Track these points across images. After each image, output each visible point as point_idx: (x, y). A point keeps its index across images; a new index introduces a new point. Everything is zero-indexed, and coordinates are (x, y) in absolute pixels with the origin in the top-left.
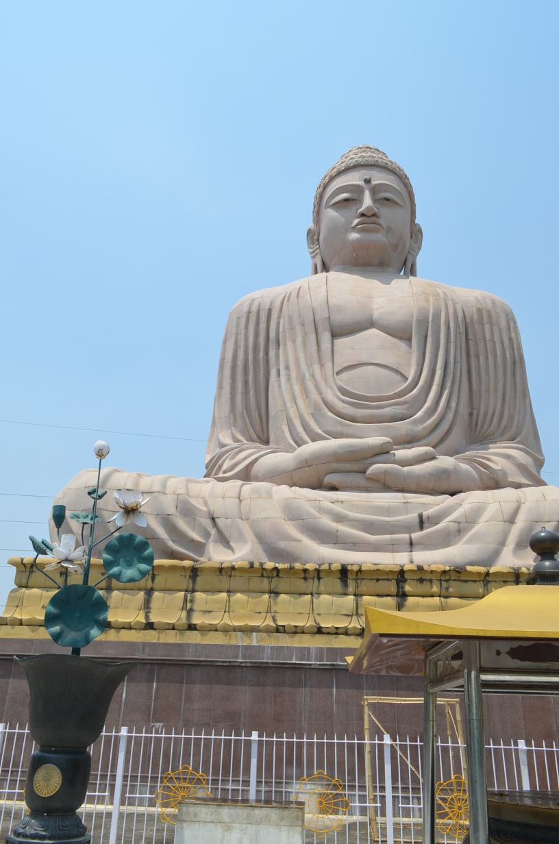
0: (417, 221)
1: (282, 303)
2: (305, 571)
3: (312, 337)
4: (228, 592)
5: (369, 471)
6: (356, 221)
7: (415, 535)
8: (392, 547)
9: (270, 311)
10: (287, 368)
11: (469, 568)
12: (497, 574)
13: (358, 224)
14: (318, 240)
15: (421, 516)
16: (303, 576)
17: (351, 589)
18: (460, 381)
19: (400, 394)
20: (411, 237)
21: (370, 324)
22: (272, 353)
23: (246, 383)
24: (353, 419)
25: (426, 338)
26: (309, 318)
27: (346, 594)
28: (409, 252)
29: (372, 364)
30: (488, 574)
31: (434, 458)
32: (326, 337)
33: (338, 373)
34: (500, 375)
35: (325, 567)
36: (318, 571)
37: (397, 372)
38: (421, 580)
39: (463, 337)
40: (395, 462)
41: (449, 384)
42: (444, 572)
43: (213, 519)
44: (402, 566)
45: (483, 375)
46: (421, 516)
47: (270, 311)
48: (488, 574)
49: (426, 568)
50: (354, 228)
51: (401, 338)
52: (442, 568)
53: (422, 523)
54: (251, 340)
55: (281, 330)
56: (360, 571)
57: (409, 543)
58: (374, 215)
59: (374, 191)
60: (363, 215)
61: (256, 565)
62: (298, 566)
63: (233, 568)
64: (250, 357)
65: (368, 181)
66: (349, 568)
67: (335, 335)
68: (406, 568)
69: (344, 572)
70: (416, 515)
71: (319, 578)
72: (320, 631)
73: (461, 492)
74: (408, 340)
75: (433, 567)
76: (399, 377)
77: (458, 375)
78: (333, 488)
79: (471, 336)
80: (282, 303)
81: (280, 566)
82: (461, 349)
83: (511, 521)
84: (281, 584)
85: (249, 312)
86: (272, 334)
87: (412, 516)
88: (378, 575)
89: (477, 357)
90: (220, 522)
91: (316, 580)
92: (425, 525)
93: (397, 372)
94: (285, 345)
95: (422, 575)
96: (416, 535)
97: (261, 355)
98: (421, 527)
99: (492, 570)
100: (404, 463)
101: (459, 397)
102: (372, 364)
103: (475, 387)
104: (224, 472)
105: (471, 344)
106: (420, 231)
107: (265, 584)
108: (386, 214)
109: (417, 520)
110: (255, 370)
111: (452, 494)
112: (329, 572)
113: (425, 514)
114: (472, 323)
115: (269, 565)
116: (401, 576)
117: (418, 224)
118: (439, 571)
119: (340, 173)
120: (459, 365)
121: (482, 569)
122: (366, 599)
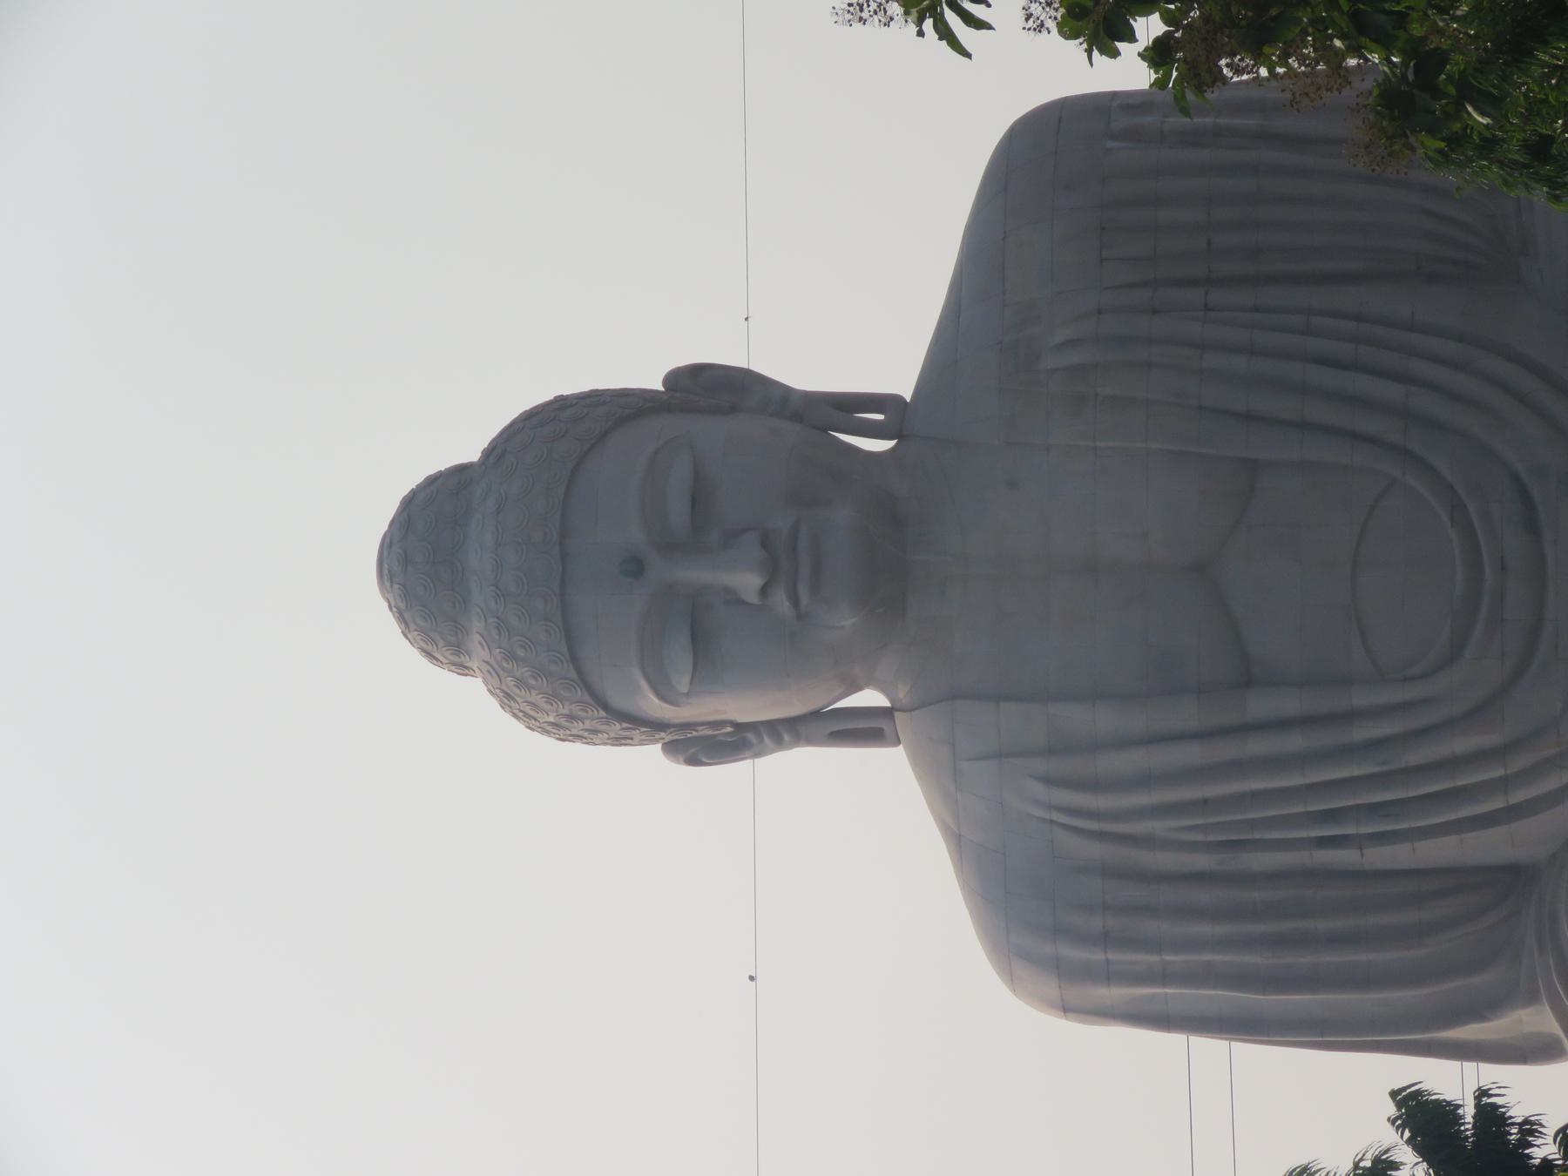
0: (652, 380)
1: (1101, 836)
3: (1257, 746)
6: (781, 602)
13: (795, 600)
14: (739, 727)
18: (1359, 318)
20: (733, 409)
23: (1336, 940)
25: (1249, 417)
26: (1192, 754)
28: (797, 417)
32: (1260, 705)
47: (1111, 872)
50: (799, 617)
55: (1199, 837)
58: (765, 542)
60: (764, 591)
65: (635, 567)
67: (1248, 678)
80: (1101, 836)
85: (1105, 939)
86: (1202, 862)
94: (1252, 824)
97: (1257, 895)
106: (697, 371)
119: (574, 659)
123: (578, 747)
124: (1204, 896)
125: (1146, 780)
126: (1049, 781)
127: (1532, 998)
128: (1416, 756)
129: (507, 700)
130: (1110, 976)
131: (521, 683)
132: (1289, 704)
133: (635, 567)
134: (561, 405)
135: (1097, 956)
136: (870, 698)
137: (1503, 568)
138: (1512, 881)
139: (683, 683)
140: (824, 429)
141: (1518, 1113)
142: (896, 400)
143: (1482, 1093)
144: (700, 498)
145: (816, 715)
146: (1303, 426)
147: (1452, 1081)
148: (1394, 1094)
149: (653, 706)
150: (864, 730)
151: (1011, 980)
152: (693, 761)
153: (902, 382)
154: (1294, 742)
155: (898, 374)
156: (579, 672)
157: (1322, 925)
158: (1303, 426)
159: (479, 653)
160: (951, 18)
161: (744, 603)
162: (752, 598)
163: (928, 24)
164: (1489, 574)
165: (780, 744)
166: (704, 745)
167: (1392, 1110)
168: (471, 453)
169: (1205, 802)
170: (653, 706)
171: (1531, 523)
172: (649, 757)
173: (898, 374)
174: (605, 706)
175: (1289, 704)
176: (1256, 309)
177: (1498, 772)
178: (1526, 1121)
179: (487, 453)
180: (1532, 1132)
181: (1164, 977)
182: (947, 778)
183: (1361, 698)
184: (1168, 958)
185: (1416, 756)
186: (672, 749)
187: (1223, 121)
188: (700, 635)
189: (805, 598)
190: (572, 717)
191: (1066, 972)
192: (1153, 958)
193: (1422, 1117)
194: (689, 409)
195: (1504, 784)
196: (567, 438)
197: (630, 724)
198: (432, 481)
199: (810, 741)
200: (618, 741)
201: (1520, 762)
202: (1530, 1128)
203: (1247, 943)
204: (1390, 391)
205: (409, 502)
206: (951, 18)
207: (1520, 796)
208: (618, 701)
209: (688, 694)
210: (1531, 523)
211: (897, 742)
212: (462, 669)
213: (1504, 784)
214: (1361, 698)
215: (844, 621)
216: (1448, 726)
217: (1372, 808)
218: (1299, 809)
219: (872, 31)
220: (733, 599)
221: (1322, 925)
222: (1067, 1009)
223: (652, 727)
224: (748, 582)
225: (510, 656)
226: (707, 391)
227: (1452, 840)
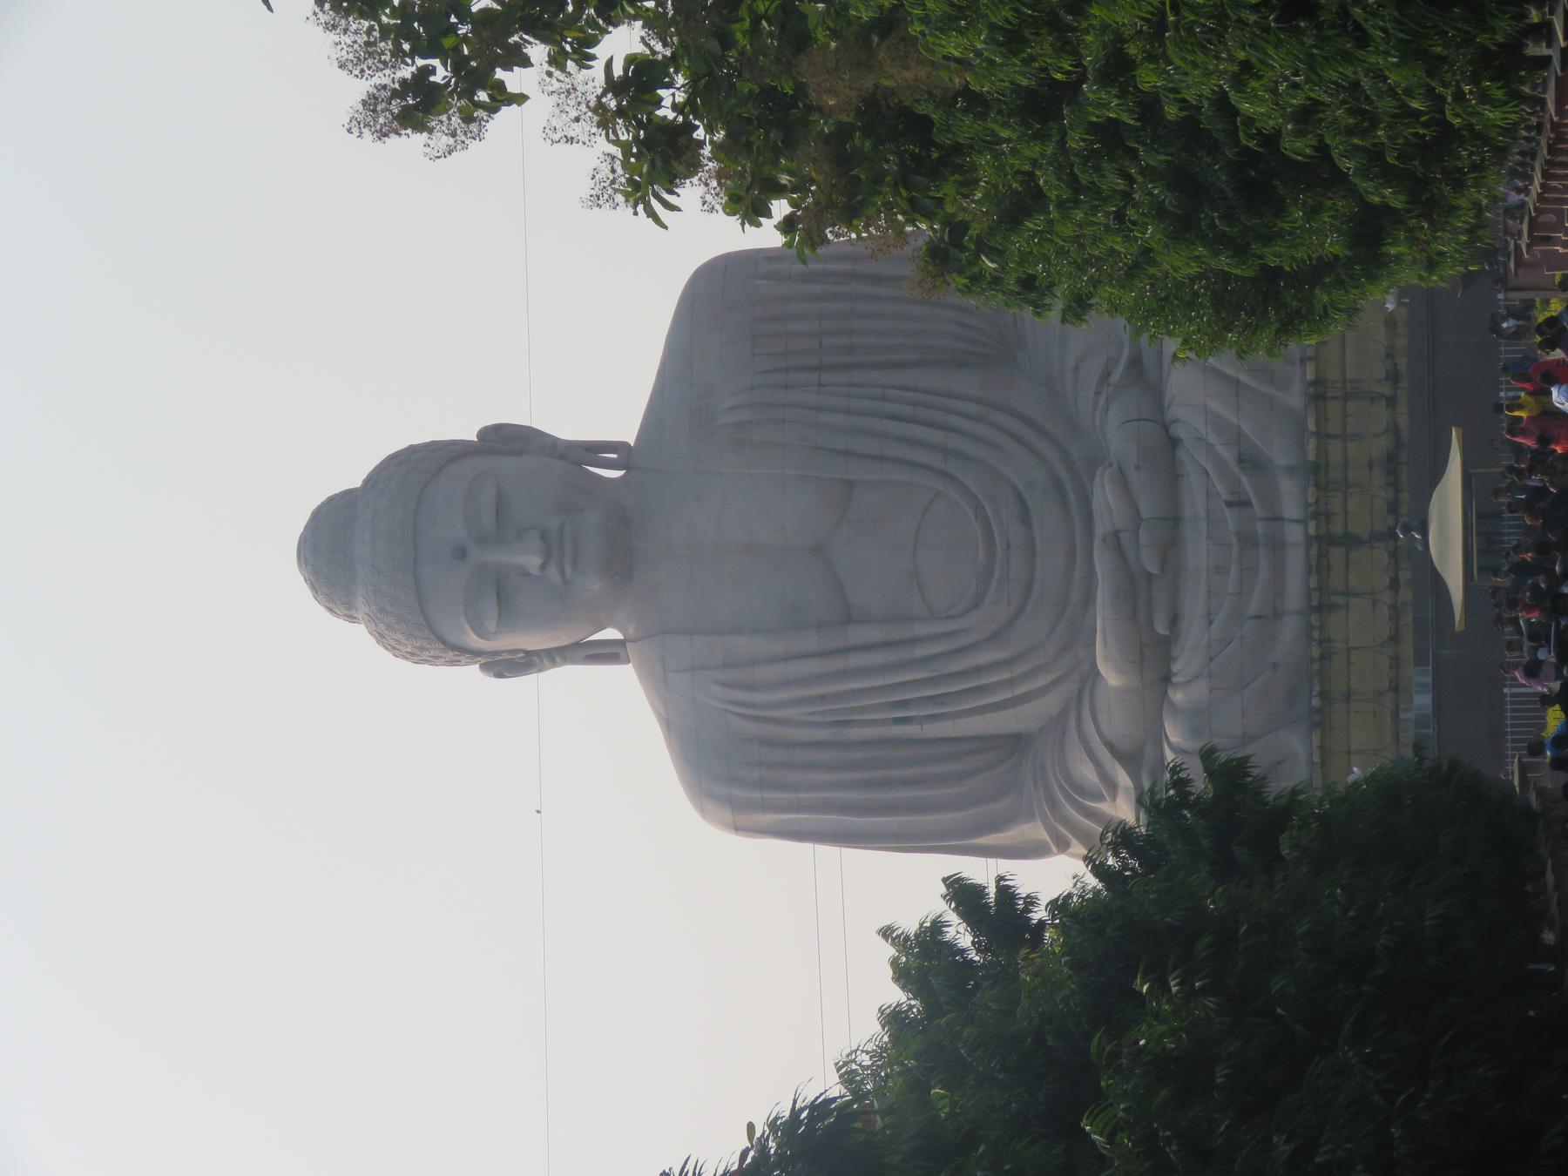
0: (468, 432)
1: (757, 719)
2: (1322, 657)
3: (855, 660)
4: (1349, 752)
5: (1154, 570)
6: (553, 573)
7: (1258, 510)
8: (1277, 546)
10: (903, 704)
11: (1312, 457)
12: (1317, 425)
13: (562, 572)
14: (528, 653)
15: (1229, 504)
17: (1340, 600)
18: (915, 390)
19: (978, 508)
20: (522, 452)
22: (856, 733)
23: (907, 783)
24: (1028, 588)
25: (847, 453)
26: (814, 666)
27: (1347, 606)
28: (562, 457)
30: (1317, 434)
32: (857, 635)
35: (1316, 634)
36: (1320, 642)
40: (1136, 532)
42: (1317, 485)
44: (1309, 540)
48: (1317, 434)
49: (1312, 509)
50: (566, 582)
52: (1311, 490)
53: (1239, 503)
54: (823, 777)
56: (1319, 589)
58: (543, 537)
60: (543, 567)
61: (1317, 718)
62: (1316, 666)
63: (1322, 748)
64: (856, 776)
65: (461, 553)
66: (1315, 603)
67: (848, 620)
68: (1312, 531)
69: (1321, 606)
70: (1227, 511)
71: (1330, 640)
72: (1395, 638)
73: (1166, 428)
74: (850, 484)
75: (1311, 499)
78: (1174, 620)
80: (757, 719)
81: (1317, 689)
83: (1237, 382)
85: (761, 784)
86: (822, 734)
87: (1230, 517)
88: (1319, 567)
94: (853, 710)
95: (1320, 514)
97: (857, 755)
98: (1249, 504)
99: (1312, 427)
100: (1137, 519)
101: (949, 395)
104: (1114, 799)
111: (1174, 443)
112: (1322, 628)
113: (1225, 497)
115: (1316, 702)
116: (1323, 541)
117: (485, 433)
119: (423, 611)
120: (891, 393)
121: (1312, 444)
123: (426, 667)
124: (823, 756)
125: (786, 683)
126: (724, 685)
127: (1030, 817)
128: (956, 666)
129: (380, 637)
130: (765, 807)
131: (389, 627)
132: (874, 634)
133: (461, 553)
134: (412, 450)
135: (756, 795)
136: (611, 634)
137: (1009, 546)
138: (1016, 743)
139: (492, 625)
140: (579, 464)
141: (1023, 891)
142: (625, 445)
143: (1000, 879)
144: (501, 509)
145: (577, 645)
146: (882, 458)
147: (981, 871)
148: (944, 880)
149: (474, 641)
150: (607, 654)
151: (702, 811)
152: (499, 675)
153: (629, 434)
154: (878, 658)
155: (624, 427)
156: (426, 618)
157: (897, 773)
158: (882, 458)
159: (362, 609)
160: (655, 203)
161: (530, 575)
162: (535, 572)
163: (640, 208)
164: (999, 551)
165: (554, 664)
166: (505, 665)
167: (944, 890)
168: (357, 483)
169: (823, 697)
170: (474, 641)
171: (1026, 519)
172: (471, 673)
173: (624, 427)
174: (444, 642)
175: (874, 634)
176: (851, 385)
177: (1007, 676)
178: (1028, 896)
179: (366, 482)
180: (1032, 904)
181: (798, 807)
182: (660, 683)
183: (921, 630)
184: (802, 795)
185: (956, 666)
186: (485, 667)
187: (831, 266)
188: (502, 596)
189: (568, 571)
190: (422, 649)
191: (736, 805)
192: (792, 796)
193: (963, 894)
195: (1011, 683)
196: (416, 474)
197: (459, 653)
198: (331, 500)
199: (573, 662)
200: (451, 663)
201: (1020, 669)
202: (1031, 901)
203: (851, 785)
204: (937, 436)
205: (316, 514)
206: (655, 203)
207: (1020, 690)
208: (451, 638)
209: (495, 633)
210: (1026, 519)
211: (628, 661)
212: (352, 619)
213: (1011, 683)
214: (921, 630)
215: (593, 585)
217: (928, 699)
218: (882, 700)
219: (606, 212)
220: (524, 573)
221: (897, 773)
222: (737, 829)
223: (473, 654)
224: (533, 562)
225: (382, 610)
226: (505, 441)
227: (977, 719)
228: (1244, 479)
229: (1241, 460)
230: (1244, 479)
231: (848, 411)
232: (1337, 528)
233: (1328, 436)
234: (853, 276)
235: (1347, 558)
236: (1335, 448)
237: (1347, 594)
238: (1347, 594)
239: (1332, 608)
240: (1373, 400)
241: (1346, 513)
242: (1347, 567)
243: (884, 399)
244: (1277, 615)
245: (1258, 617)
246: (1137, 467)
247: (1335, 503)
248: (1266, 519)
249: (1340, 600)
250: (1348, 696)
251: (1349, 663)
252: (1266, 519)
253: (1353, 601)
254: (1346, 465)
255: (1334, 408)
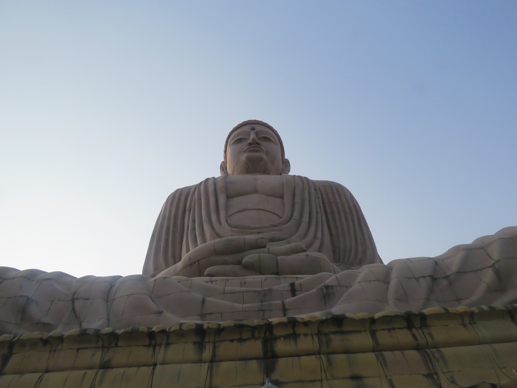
9: (188, 194)
15: (292, 285)
16: (147, 342)
17: (207, 354)
20: (283, 163)
21: (256, 191)
23: (167, 240)
25: (294, 196)
27: (201, 361)
28: (282, 171)
29: (255, 209)
31: (305, 251)
33: (229, 216)
34: (351, 223)
37: (274, 213)
38: (294, 336)
39: (321, 200)
41: (314, 223)
43: (73, 300)
45: (338, 224)
46: (292, 285)
50: (245, 151)
51: (276, 197)
53: (293, 290)
57: (282, 308)
58: (258, 143)
59: (257, 134)
60: (250, 144)
63: (60, 339)
67: (229, 197)
71: (168, 345)
74: (282, 197)
76: (275, 217)
77: (320, 220)
79: (326, 201)
82: (320, 207)
84: (119, 355)
89: (332, 213)
90: (77, 304)
91: (163, 347)
92: (297, 293)
93: (274, 213)
94: (195, 209)
96: (289, 300)
97: (179, 221)
98: (294, 295)
100: (277, 254)
102: (255, 209)
103: (334, 232)
105: (327, 206)
107: (97, 357)
108: (265, 145)
109: (289, 288)
110: (173, 231)
113: (297, 282)
114: (327, 194)
118: (314, 320)
122: (224, 365)
133: (253, 129)
169: (201, 199)
183: (222, 214)
186: (223, 162)
194: (283, 161)
215: (243, 157)
216: (213, 227)
228: (315, 290)
229: (327, 287)
230: (315, 290)
231: (310, 201)
232: (281, 346)
233: (373, 334)
234: (359, 219)
235: (251, 359)
236: (364, 339)
237: (213, 360)
238: (213, 360)
239: (200, 346)
240: (429, 376)
241: (299, 356)
242: (242, 359)
243: (317, 213)
244: (203, 316)
245: (204, 301)
246: (307, 255)
247: (307, 343)
248: (283, 304)
249: (207, 354)
250: (106, 366)
251: (139, 366)
252: (283, 304)
253: (206, 365)
254: (347, 352)
255: (404, 336)
